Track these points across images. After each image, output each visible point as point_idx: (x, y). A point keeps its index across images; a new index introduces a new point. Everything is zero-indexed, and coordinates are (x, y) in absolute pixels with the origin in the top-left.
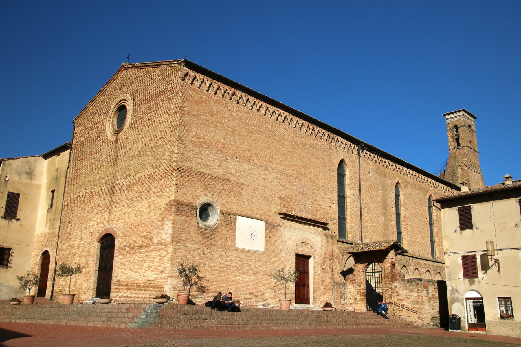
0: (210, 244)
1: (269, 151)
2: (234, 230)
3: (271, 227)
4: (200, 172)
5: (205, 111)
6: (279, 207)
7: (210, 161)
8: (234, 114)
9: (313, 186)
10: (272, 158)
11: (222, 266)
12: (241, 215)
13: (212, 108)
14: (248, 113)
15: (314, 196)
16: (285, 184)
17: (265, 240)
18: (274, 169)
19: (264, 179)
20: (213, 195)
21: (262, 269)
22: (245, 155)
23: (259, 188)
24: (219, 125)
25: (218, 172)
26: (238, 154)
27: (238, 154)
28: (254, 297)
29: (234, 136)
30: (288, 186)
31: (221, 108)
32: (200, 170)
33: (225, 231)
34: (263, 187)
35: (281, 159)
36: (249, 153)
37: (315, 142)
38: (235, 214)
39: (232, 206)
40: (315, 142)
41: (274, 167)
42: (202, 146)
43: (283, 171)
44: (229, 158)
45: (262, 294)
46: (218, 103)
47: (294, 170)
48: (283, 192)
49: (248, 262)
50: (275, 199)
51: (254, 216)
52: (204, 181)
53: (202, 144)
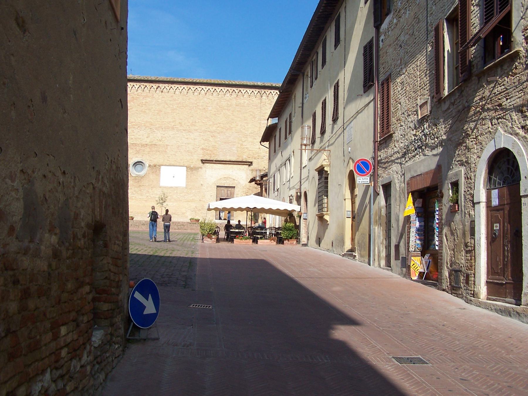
0: (140, 186)
1: (192, 118)
2: (159, 175)
3: (190, 169)
4: (133, 144)
5: (136, 105)
6: (202, 156)
7: (140, 135)
8: (160, 101)
9: (239, 135)
10: (195, 122)
11: (150, 198)
12: (166, 165)
13: (142, 101)
14: (172, 96)
15: (241, 142)
16: (208, 138)
17: (187, 179)
18: (197, 130)
19: (187, 138)
20: (143, 156)
21: (183, 198)
22: (170, 126)
23: (182, 146)
24: (147, 111)
25: (148, 141)
26: (164, 126)
27: (164, 126)
28: (176, 216)
29: (160, 115)
30: (211, 139)
31: (148, 99)
32: (133, 142)
33: (152, 177)
34: (186, 144)
35: (204, 121)
36: (173, 124)
37: (242, 101)
38: (160, 166)
39: (157, 159)
40: (242, 101)
41: (196, 128)
42: (134, 127)
43: (206, 129)
44: (156, 131)
45: (183, 213)
46: (147, 96)
47: (218, 127)
48: (206, 145)
49: (171, 194)
50: (197, 151)
51: (178, 164)
52: (135, 148)
53: (134, 126)
